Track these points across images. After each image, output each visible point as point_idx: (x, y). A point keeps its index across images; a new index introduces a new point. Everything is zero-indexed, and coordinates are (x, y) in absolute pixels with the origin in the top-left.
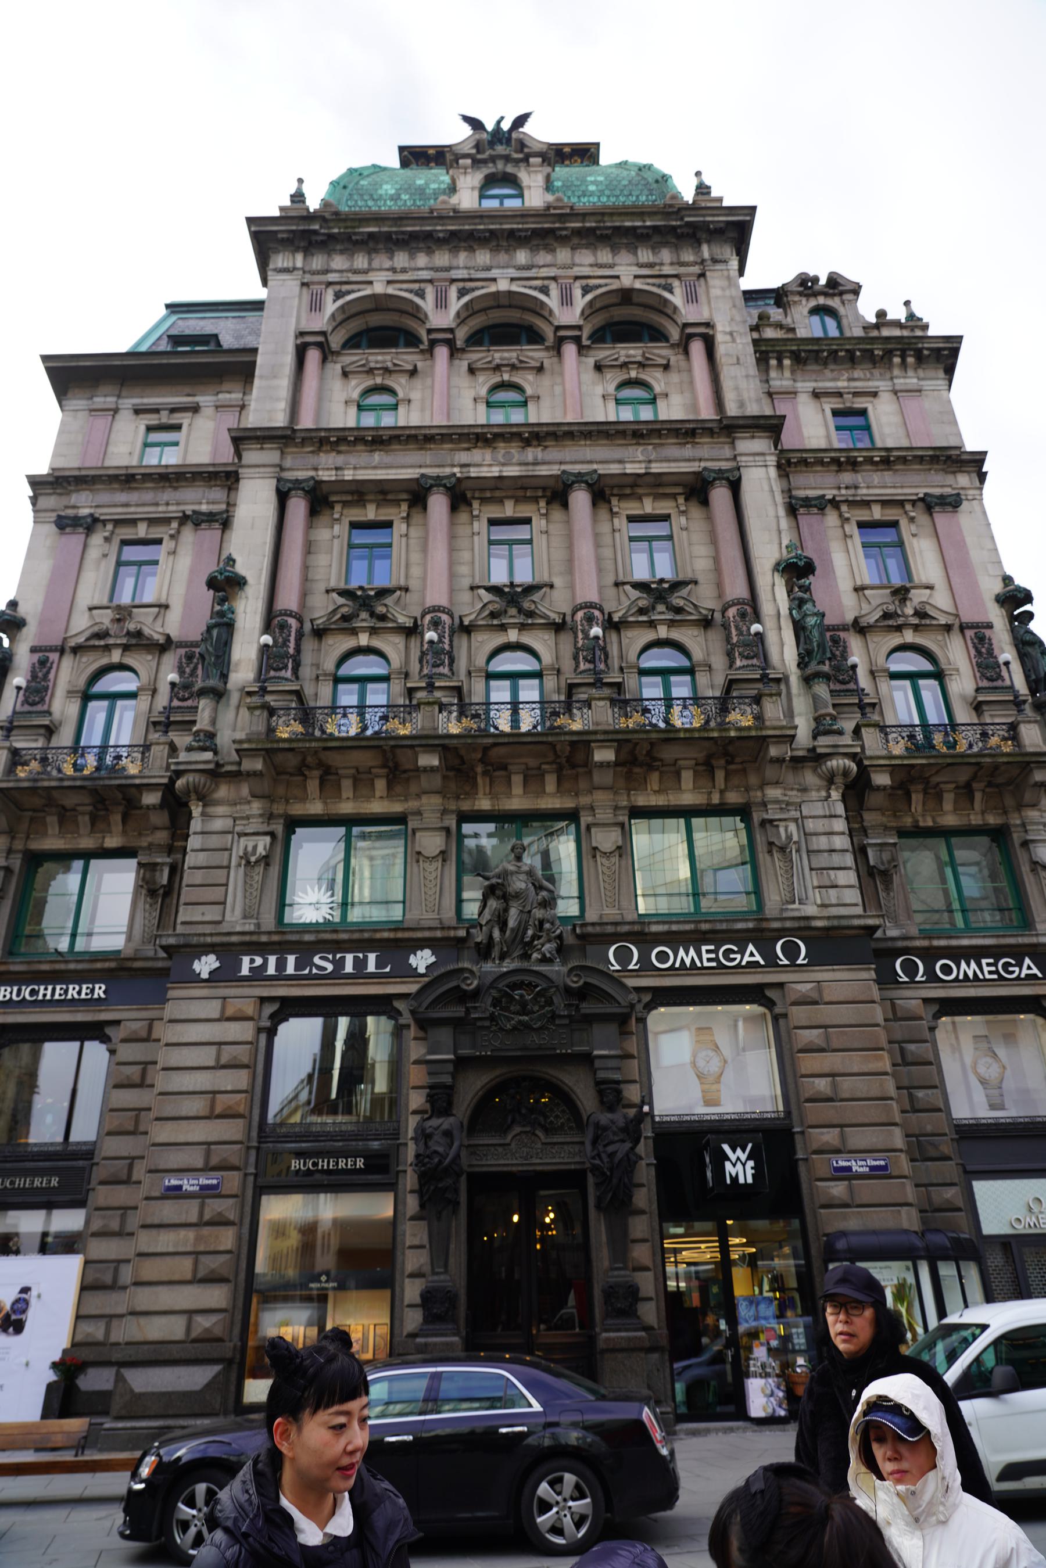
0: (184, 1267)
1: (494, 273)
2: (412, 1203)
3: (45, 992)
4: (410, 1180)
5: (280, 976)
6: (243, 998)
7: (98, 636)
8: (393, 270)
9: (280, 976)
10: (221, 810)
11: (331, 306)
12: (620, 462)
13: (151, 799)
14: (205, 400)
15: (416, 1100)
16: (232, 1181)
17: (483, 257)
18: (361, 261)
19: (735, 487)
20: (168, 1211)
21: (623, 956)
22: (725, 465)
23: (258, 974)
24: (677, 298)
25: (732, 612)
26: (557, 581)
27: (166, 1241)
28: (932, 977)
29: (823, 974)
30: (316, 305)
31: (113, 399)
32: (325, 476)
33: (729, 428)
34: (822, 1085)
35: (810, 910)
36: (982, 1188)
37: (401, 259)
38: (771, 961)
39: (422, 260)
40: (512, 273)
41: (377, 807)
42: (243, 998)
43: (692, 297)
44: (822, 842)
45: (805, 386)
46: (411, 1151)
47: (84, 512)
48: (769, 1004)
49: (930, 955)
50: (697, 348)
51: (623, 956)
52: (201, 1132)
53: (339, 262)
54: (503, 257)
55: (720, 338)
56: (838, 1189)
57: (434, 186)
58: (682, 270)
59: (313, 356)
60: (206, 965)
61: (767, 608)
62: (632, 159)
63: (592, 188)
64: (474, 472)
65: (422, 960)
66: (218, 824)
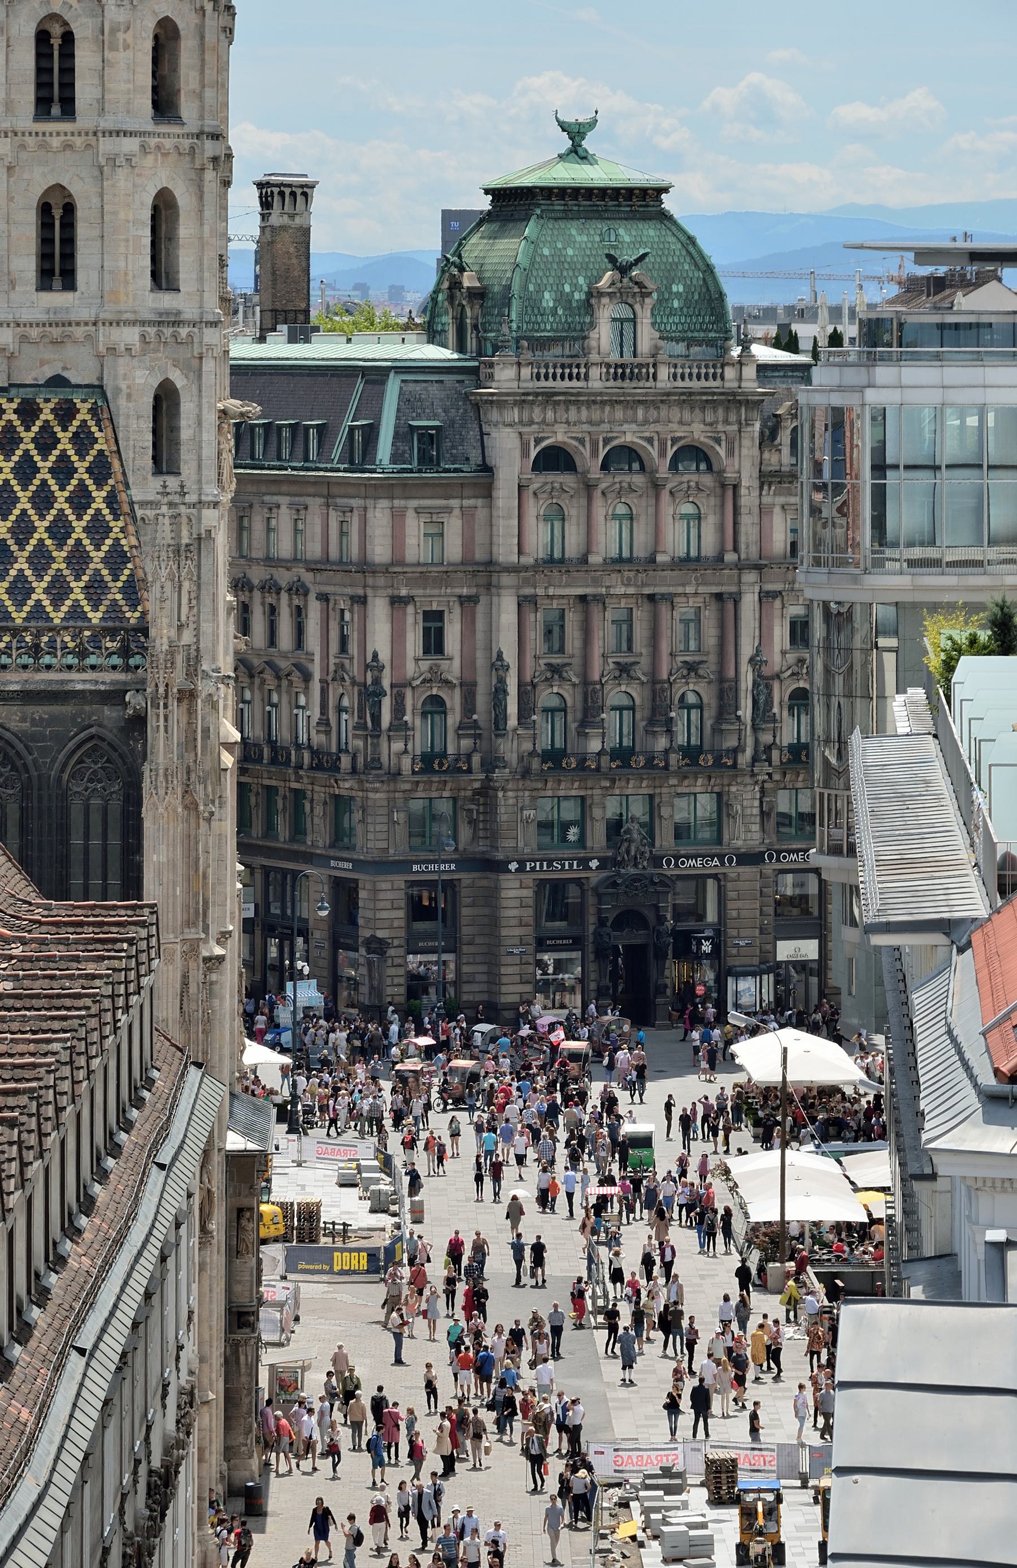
0: (517, 978)
1: (626, 427)
2: (592, 957)
3: (431, 867)
4: (590, 948)
5: (541, 870)
6: (529, 879)
7: (424, 681)
8: (568, 422)
9: (541, 870)
10: (510, 794)
11: (533, 454)
12: (684, 585)
13: (477, 785)
14: (455, 503)
15: (592, 919)
16: (531, 949)
17: (619, 414)
18: (550, 415)
19: (737, 603)
20: (509, 960)
21: (669, 863)
22: (733, 589)
23: (533, 869)
24: (722, 452)
25: (726, 685)
26: (644, 651)
27: (510, 970)
28: (778, 860)
29: (741, 869)
30: (525, 453)
31: (403, 503)
32: (540, 591)
33: (740, 567)
34: (734, 914)
35: (740, 843)
36: (780, 944)
37: (573, 414)
38: (723, 864)
39: (584, 413)
40: (634, 426)
41: (573, 793)
42: (529, 879)
43: (730, 452)
44: (748, 811)
45: (781, 500)
46: (591, 939)
47: (404, 592)
48: (719, 880)
49: (779, 852)
50: (730, 493)
51: (669, 863)
52: (518, 931)
53: (537, 414)
54: (630, 412)
55: (743, 491)
56: (734, 951)
57: (577, 296)
58: (729, 428)
59: (525, 494)
60: (513, 866)
61: (743, 687)
62: (699, 241)
63: (676, 304)
64: (612, 591)
65: (594, 864)
66: (511, 802)
